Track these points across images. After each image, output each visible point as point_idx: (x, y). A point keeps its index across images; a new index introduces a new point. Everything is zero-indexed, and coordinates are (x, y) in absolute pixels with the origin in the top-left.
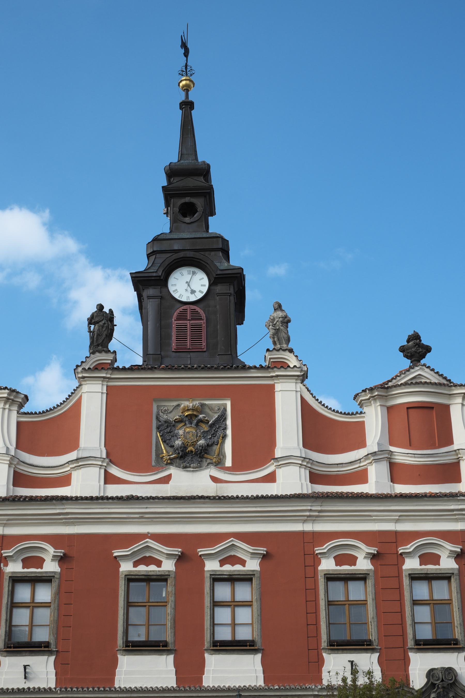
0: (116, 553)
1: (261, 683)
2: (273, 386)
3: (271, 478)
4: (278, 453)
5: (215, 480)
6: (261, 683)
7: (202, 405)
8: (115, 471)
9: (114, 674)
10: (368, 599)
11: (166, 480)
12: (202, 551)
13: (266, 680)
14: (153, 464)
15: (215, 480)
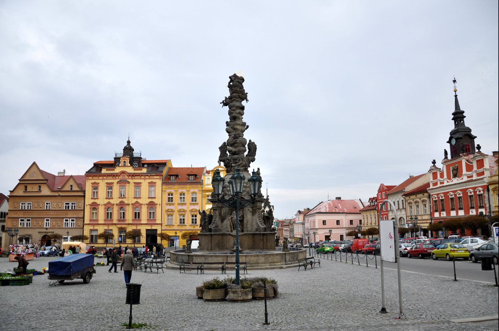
0: (448, 195)
1: (464, 215)
2: (462, 161)
3: (462, 179)
4: (463, 174)
5: (457, 180)
6: (464, 215)
7: (455, 166)
8: (448, 180)
9: (450, 214)
10: (445, 209)
11: (452, 181)
12: (456, 193)
13: (465, 214)
14: (452, 178)
15: (457, 180)
